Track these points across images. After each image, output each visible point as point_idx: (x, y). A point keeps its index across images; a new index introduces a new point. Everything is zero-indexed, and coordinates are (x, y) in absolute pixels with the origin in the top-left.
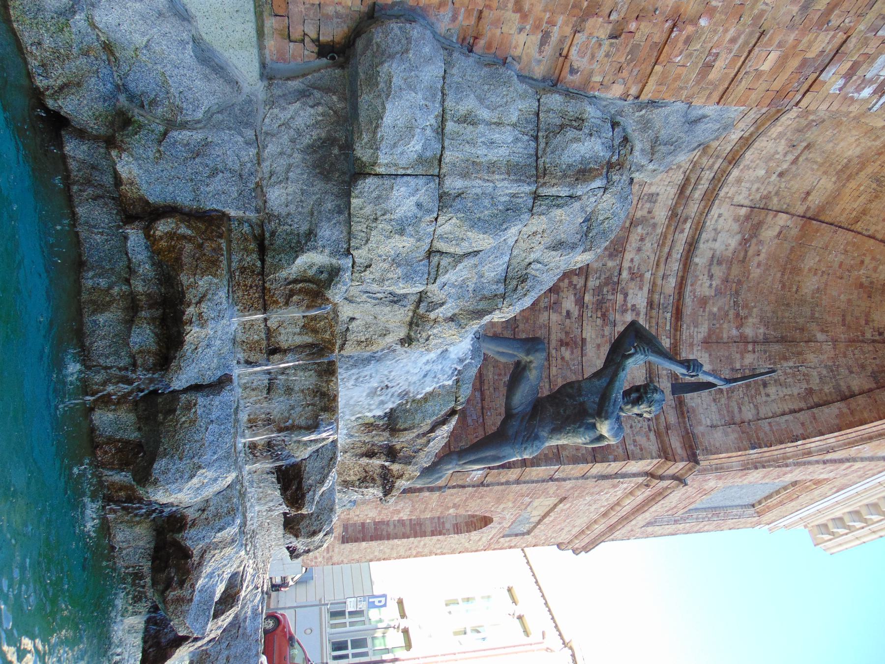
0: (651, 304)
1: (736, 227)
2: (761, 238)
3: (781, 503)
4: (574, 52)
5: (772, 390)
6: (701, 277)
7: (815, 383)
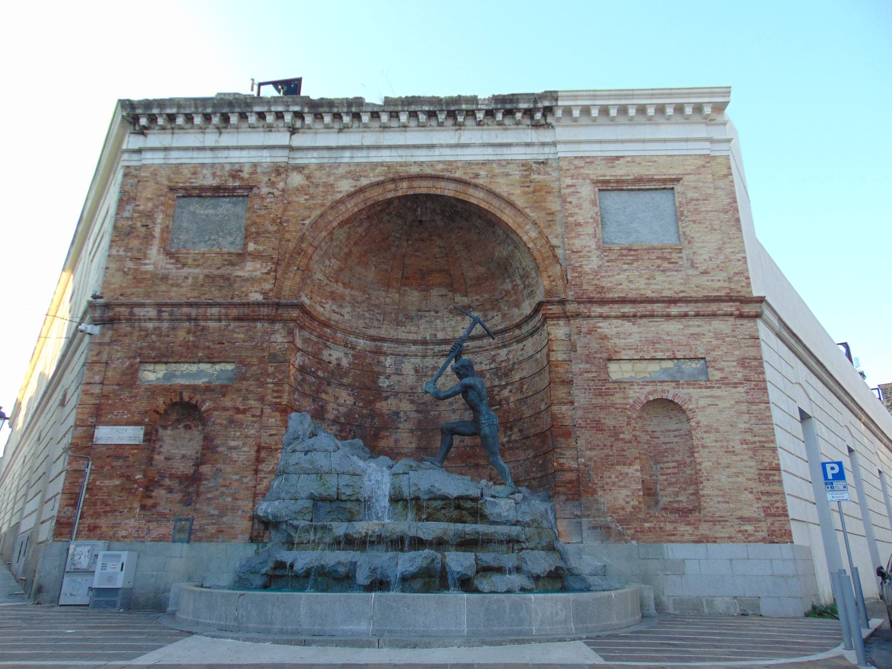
0: (505, 346)
3: (651, 180)
7: (511, 247)
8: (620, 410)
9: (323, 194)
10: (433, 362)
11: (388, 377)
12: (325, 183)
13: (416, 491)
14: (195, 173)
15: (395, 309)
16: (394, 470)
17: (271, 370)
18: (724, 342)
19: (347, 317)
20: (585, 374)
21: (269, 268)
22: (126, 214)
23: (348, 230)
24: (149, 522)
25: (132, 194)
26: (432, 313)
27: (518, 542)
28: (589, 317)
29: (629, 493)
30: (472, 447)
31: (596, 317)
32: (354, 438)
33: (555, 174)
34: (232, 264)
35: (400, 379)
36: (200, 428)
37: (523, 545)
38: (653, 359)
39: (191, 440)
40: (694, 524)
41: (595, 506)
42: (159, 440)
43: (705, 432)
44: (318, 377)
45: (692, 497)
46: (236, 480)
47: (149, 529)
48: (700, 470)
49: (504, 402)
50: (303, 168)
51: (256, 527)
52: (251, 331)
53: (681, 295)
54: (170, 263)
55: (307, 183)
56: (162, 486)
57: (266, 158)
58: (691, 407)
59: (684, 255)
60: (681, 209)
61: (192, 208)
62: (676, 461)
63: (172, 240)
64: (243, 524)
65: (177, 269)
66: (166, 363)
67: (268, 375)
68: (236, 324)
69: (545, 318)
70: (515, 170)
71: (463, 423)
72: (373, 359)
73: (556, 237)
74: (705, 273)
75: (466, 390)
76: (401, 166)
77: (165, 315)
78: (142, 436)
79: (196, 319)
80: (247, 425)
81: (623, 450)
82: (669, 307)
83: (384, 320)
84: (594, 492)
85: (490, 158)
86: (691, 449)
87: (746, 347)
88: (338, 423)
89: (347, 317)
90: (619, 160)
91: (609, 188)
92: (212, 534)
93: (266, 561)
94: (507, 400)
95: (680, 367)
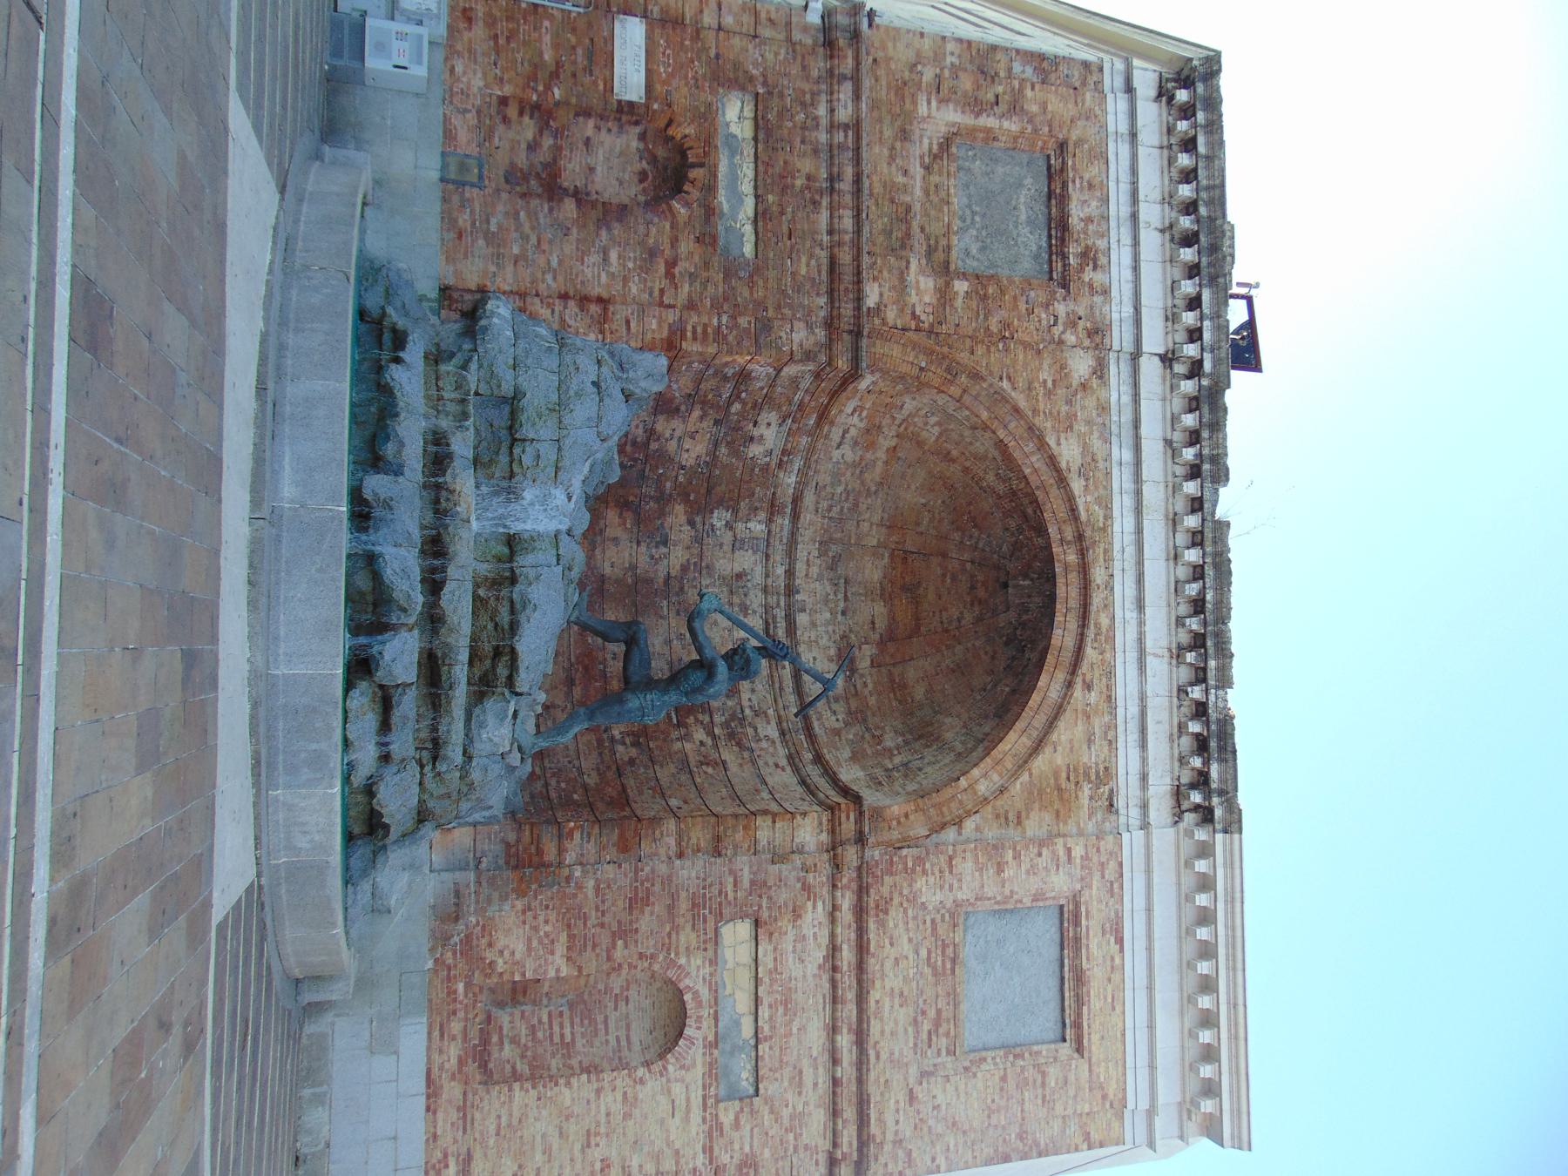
0: (783, 733)
3: (1080, 1001)
7: (959, 747)
8: (667, 941)
9: (1055, 412)
10: (755, 606)
11: (729, 526)
12: (1076, 415)
13: (526, 577)
14: (1091, 186)
15: (850, 538)
16: (564, 539)
17: (743, 321)
18: (786, 1130)
19: (836, 454)
20: (731, 880)
21: (923, 317)
22: (1017, 67)
23: (990, 455)
24: (479, 112)
25: (1053, 77)
26: (842, 605)
27: (435, 759)
28: (834, 886)
29: (518, 956)
30: (604, 675)
31: (834, 898)
32: (622, 466)
33: (1090, 827)
34: (930, 252)
35: (725, 547)
36: (642, 198)
37: (428, 769)
38: (757, 1001)
39: (621, 184)
40: (460, 1071)
41: (496, 895)
42: (621, 127)
43: (625, 1093)
44: (729, 404)
45: (508, 1068)
46: (549, 262)
47: (466, 111)
48: (556, 1085)
49: (683, 731)
50: (1101, 377)
51: (468, 297)
52: (812, 287)
53: (872, 1053)
54: (931, 144)
55: (1075, 383)
56: (541, 132)
57: (1119, 311)
58: (671, 1068)
59: (944, 1058)
60: (1027, 1055)
61: (1028, 181)
62: (573, 1040)
63: (972, 148)
64: (472, 273)
65: (922, 157)
66: (755, 139)
67: (733, 317)
68: (825, 261)
69: (832, 808)
70: (1097, 756)
71: (646, 663)
72: (761, 500)
73: (977, 829)
74: (912, 1097)
75: (704, 666)
76: (1106, 551)
77: (839, 137)
78: (627, 98)
79: (832, 189)
80: (645, 280)
81: (594, 946)
82: (849, 1030)
83: (830, 518)
84: (521, 894)
85: (1120, 711)
86: (596, 1068)
87: (777, 1170)
88: (648, 439)
89: (836, 454)
90: (1116, 943)
91: (1066, 925)
92: (456, 221)
93: (407, 315)
94: (687, 737)
95: (741, 1049)
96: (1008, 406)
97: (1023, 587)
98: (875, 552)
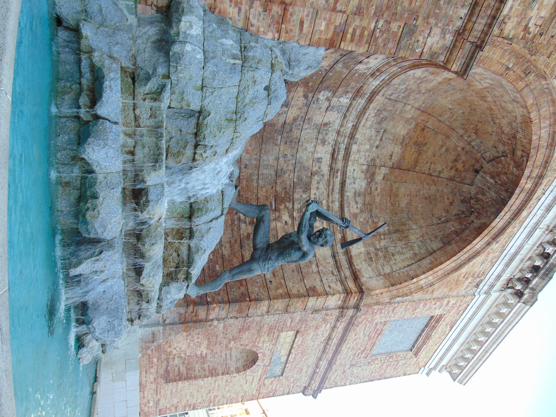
1: (363, 176)
2: (376, 181)
3: (424, 343)
4: (251, 17)
5: (397, 257)
6: (351, 203)
7: (416, 249)
11: (328, 99)
13: (200, 232)
15: (396, 111)
17: (394, 26)
20: (290, 320)
35: (322, 110)
45: (177, 369)
49: (277, 214)
67: (388, 23)
69: (347, 292)
81: (220, 344)
96: (550, 98)
97: (488, 181)
98: (407, 121)
